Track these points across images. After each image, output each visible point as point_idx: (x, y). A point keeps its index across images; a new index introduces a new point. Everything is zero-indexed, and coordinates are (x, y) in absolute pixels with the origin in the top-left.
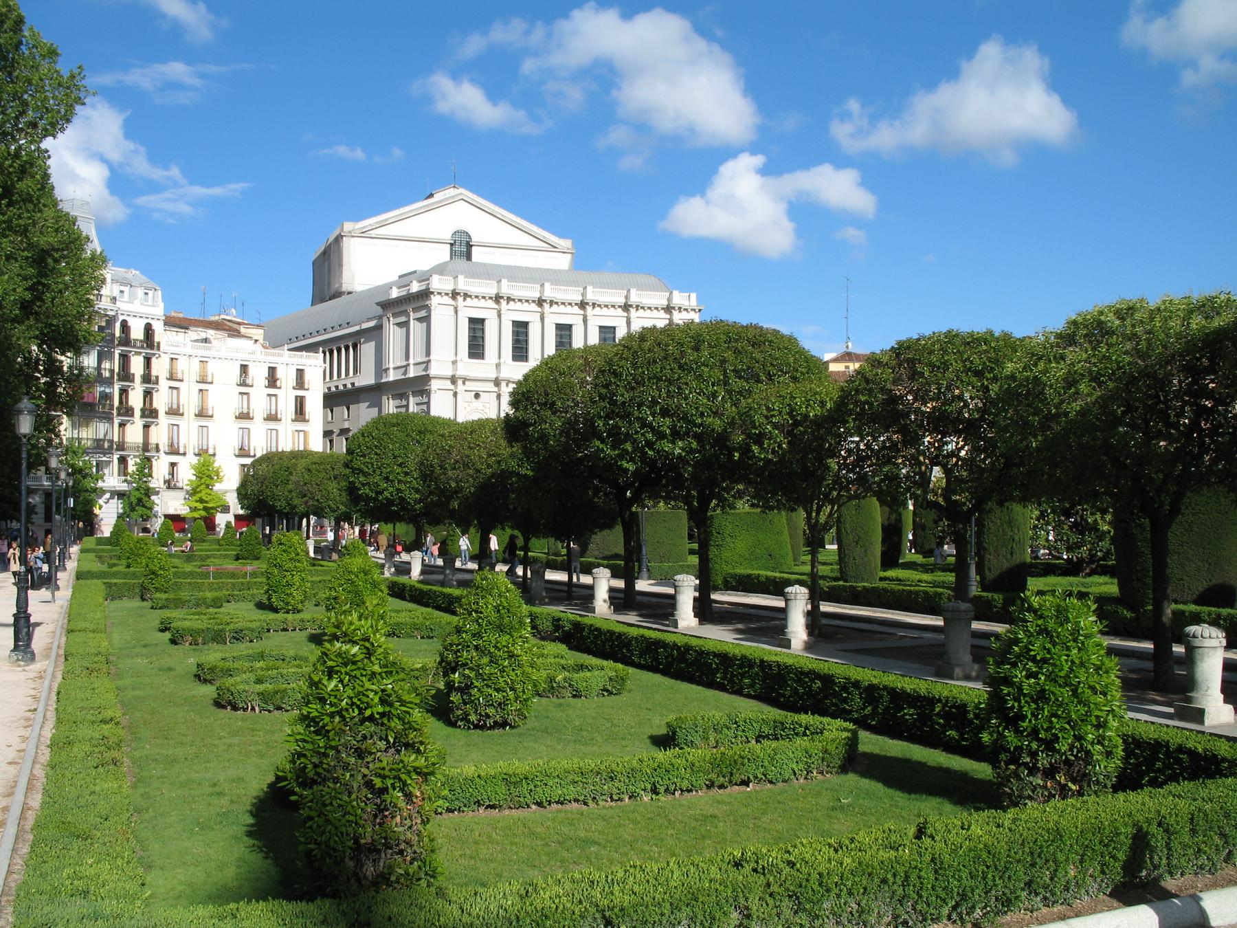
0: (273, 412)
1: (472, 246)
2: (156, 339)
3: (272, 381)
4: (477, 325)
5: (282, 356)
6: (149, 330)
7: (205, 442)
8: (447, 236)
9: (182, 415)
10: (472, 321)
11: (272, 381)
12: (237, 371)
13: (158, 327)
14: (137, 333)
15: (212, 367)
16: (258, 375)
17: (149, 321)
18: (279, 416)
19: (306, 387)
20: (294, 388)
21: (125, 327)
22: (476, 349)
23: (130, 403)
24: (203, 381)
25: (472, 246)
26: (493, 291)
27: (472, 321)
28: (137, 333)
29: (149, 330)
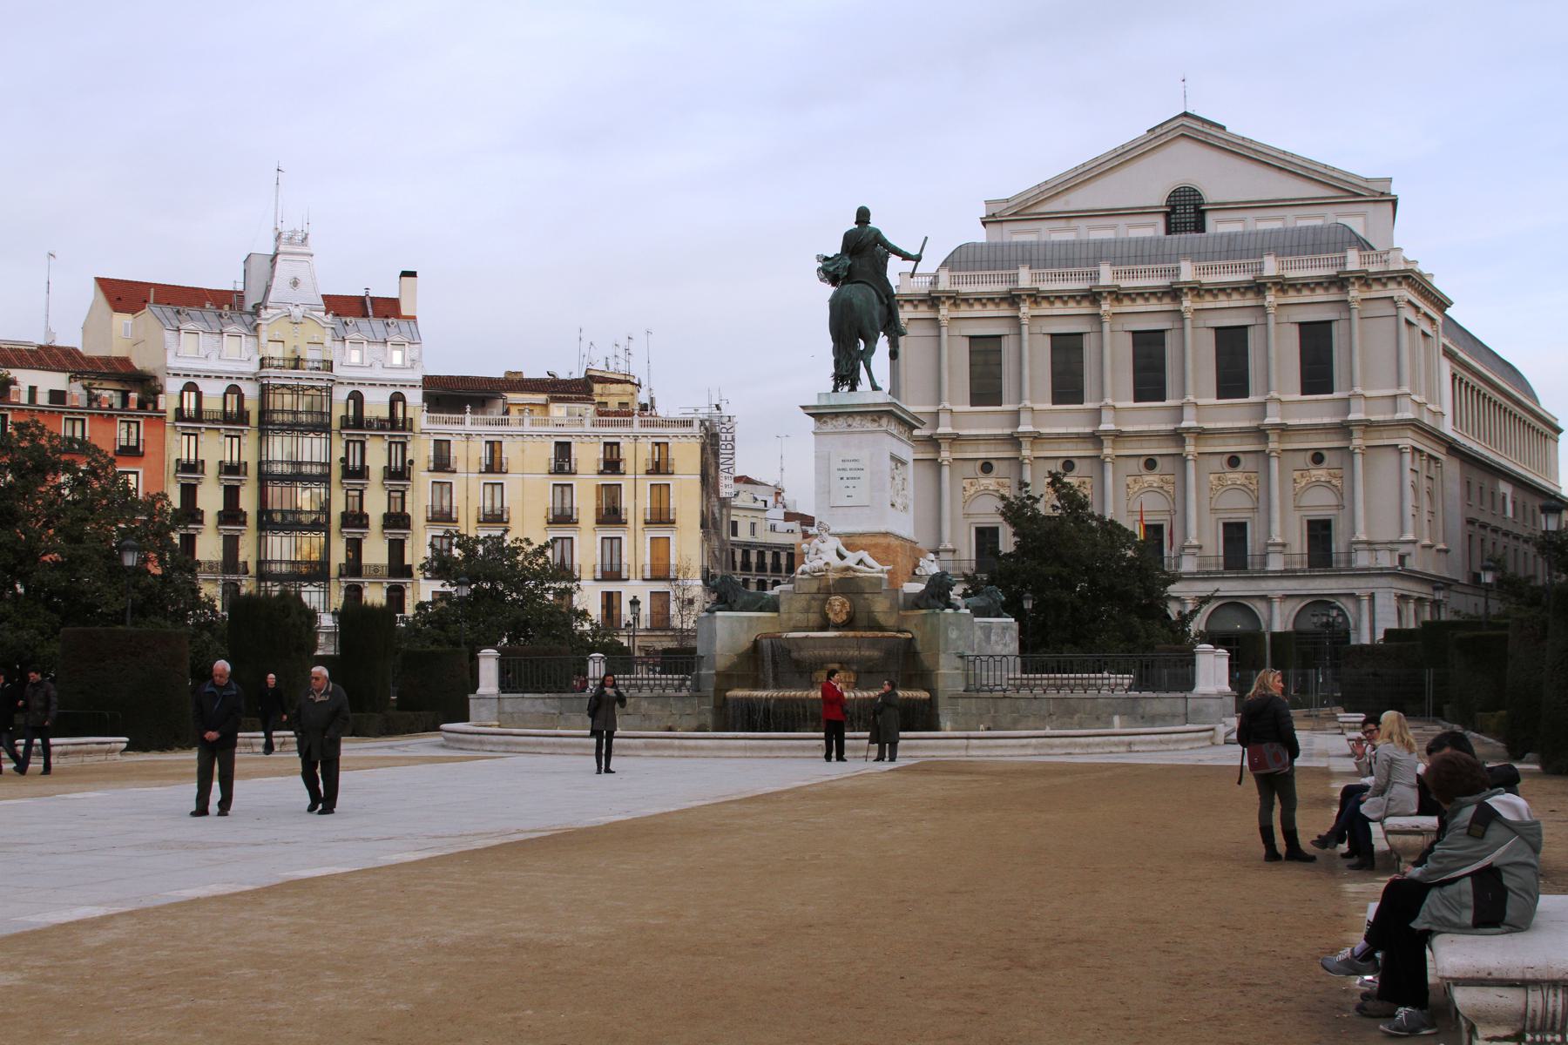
1: (1203, 212)
3: (612, 464)
4: (985, 352)
5: (631, 424)
6: (397, 398)
7: (616, 561)
8: (1158, 198)
11: (612, 464)
12: (551, 451)
15: (509, 451)
16: (588, 456)
17: (356, 388)
20: (648, 473)
21: (357, 398)
22: (986, 390)
23: (406, 511)
24: (490, 469)
25: (1203, 212)
28: (376, 404)
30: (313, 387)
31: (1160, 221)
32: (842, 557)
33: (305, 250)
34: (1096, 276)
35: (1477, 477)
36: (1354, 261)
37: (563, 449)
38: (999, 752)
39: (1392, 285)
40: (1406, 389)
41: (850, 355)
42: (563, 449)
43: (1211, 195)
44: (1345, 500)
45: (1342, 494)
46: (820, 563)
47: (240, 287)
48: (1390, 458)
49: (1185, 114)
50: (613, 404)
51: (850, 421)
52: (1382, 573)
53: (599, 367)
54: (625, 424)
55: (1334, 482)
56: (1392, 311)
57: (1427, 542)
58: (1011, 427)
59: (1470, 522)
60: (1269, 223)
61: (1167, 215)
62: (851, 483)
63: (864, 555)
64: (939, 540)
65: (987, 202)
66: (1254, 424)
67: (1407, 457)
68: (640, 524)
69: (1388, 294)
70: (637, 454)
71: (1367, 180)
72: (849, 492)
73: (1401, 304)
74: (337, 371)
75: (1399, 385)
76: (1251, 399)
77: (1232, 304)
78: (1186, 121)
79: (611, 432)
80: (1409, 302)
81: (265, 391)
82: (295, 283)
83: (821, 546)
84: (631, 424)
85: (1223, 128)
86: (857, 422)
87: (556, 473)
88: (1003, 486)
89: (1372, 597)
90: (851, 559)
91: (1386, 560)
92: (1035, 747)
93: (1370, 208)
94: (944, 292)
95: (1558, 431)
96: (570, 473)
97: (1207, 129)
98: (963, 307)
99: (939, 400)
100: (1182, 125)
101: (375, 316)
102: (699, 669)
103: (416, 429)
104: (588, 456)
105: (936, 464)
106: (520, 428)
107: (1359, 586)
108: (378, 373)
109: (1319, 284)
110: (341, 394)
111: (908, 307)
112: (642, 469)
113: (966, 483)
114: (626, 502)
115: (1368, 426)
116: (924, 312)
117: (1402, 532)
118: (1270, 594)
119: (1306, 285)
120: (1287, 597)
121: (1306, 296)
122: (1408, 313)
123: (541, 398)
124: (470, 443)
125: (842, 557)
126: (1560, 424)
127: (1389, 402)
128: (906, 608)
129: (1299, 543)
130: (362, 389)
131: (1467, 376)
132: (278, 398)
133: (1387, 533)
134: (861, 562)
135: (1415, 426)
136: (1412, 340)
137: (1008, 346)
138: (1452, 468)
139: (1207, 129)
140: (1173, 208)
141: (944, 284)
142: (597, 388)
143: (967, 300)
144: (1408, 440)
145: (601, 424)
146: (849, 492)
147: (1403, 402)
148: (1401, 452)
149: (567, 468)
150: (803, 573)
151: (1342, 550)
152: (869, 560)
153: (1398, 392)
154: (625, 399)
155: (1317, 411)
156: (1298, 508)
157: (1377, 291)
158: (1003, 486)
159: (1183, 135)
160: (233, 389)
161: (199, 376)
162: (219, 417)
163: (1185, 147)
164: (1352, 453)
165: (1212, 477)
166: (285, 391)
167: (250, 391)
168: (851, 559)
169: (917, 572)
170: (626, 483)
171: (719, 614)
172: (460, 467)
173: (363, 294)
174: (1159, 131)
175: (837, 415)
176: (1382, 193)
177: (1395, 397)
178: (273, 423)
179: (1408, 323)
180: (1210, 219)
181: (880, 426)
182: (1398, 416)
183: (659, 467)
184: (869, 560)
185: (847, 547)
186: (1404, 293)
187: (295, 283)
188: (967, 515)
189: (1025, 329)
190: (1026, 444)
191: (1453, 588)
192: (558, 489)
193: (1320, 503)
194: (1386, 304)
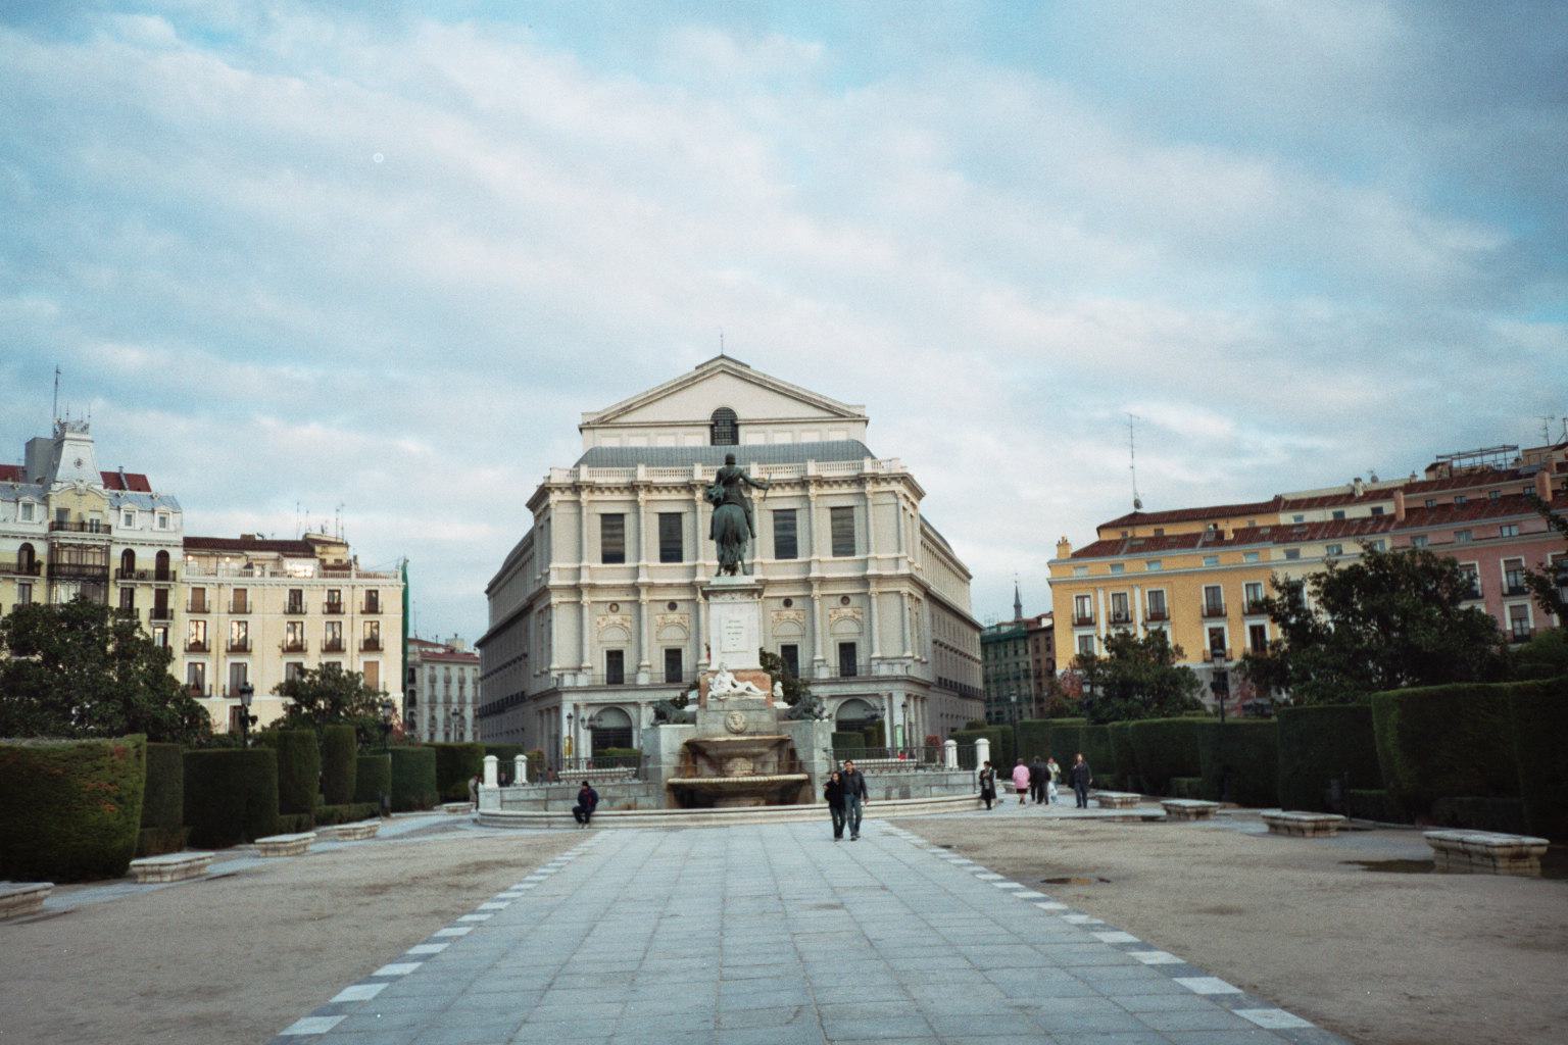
0: (333, 641)
1: (737, 426)
2: (172, 568)
3: (334, 608)
4: (612, 524)
5: (349, 576)
6: (163, 557)
8: (706, 415)
9: (209, 651)
10: (664, 517)
11: (334, 608)
12: (285, 597)
13: (176, 555)
14: (146, 560)
16: (314, 601)
18: (343, 646)
19: (380, 610)
20: (362, 612)
21: (129, 556)
26: (624, 480)
27: (664, 517)
28: (146, 560)
29: (163, 557)
30: (95, 546)
31: (707, 431)
32: (735, 686)
33: (84, 437)
34: (691, 473)
35: (938, 610)
36: (868, 467)
37: (296, 596)
38: (909, 813)
39: (894, 483)
40: (903, 554)
41: (732, 552)
42: (296, 596)
43: (742, 414)
44: (865, 628)
45: (862, 625)
46: (724, 691)
47: (22, 464)
48: (896, 600)
49: (722, 357)
50: (330, 561)
51: (734, 595)
52: (896, 680)
53: (315, 533)
54: (344, 576)
55: (857, 616)
56: (893, 500)
57: (917, 657)
58: (632, 578)
59: (935, 642)
60: (782, 437)
61: (712, 426)
62: (734, 636)
63: (749, 684)
64: (581, 659)
65: (583, 414)
66: (802, 576)
67: (906, 600)
68: (356, 652)
69: (892, 489)
70: (353, 598)
71: (849, 406)
72: (734, 642)
73: (900, 496)
74: (115, 533)
75: (899, 550)
76: (799, 560)
77: (786, 494)
78: (722, 361)
79: (333, 582)
80: (905, 496)
81: (54, 550)
82: (79, 463)
83: (723, 679)
84: (349, 576)
85: (748, 367)
86: (738, 597)
87: (290, 613)
88: (626, 620)
89: (890, 696)
90: (741, 687)
91: (898, 671)
92: (930, 808)
93: (851, 425)
94: (585, 482)
95: (970, 577)
96: (301, 613)
97: (739, 368)
98: (597, 493)
99: (580, 559)
100: (722, 365)
101: (131, 489)
102: (647, 765)
103: (178, 578)
104: (314, 601)
105: (579, 606)
106: (262, 579)
107: (883, 689)
108: (148, 536)
109: (845, 481)
110: (117, 552)
111: (557, 493)
112: (357, 610)
113: (599, 619)
114: (346, 636)
115: (879, 578)
116: (569, 496)
117: (904, 651)
118: (821, 695)
119: (836, 482)
120: (832, 697)
121: (836, 490)
122: (903, 502)
123: (274, 555)
124: (222, 591)
125: (735, 686)
126: (971, 572)
127: (892, 562)
128: (779, 719)
129: (834, 659)
130: (134, 548)
131: (928, 543)
132: (90, 556)
133: (893, 651)
134: (748, 689)
135: (911, 578)
136: (905, 518)
137: (629, 522)
138: (925, 604)
139: (739, 368)
140: (717, 424)
141: (585, 475)
142: (318, 549)
143: (601, 489)
144: (906, 588)
145: (325, 576)
146: (734, 642)
147: (903, 563)
148: (902, 596)
149: (298, 608)
150: (712, 697)
151: (863, 663)
152: (753, 687)
153: (899, 555)
154: (339, 557)
155: (844, 568)
156: (833, 634)
157: (884, 487)
158: (626, 620)
159: (723, 372)
160: (28, 550)
161: (33, 538)
162: (15, 569)
163: (724, 379)
164: (870, 598)
165: (773, 614)
166: (96, 550)
167: (41, 551)
168: (741, 687)
169: (774, 694)
170: (345, 619)
171: (662, 726)
172: (214, 608)
173: (116, 470)
174: (706, 368)
175: (724, 592)
176: (859, 416)
177: (897, 559)
178: (61, 574)
179: (904, 509)
180: (742, 430)
181: (753, 598)
182: (900, 572)
183: (372, 605)
184: (753, 687)
185: (736, 678)
186: (900, 488)
187: (79, 463)
188: (601, 642)
189: (642, 510)
190: (643, 592)
191: (931, 688)
192: (329, 626)
193: (848, 631)
194: (890, 495)
